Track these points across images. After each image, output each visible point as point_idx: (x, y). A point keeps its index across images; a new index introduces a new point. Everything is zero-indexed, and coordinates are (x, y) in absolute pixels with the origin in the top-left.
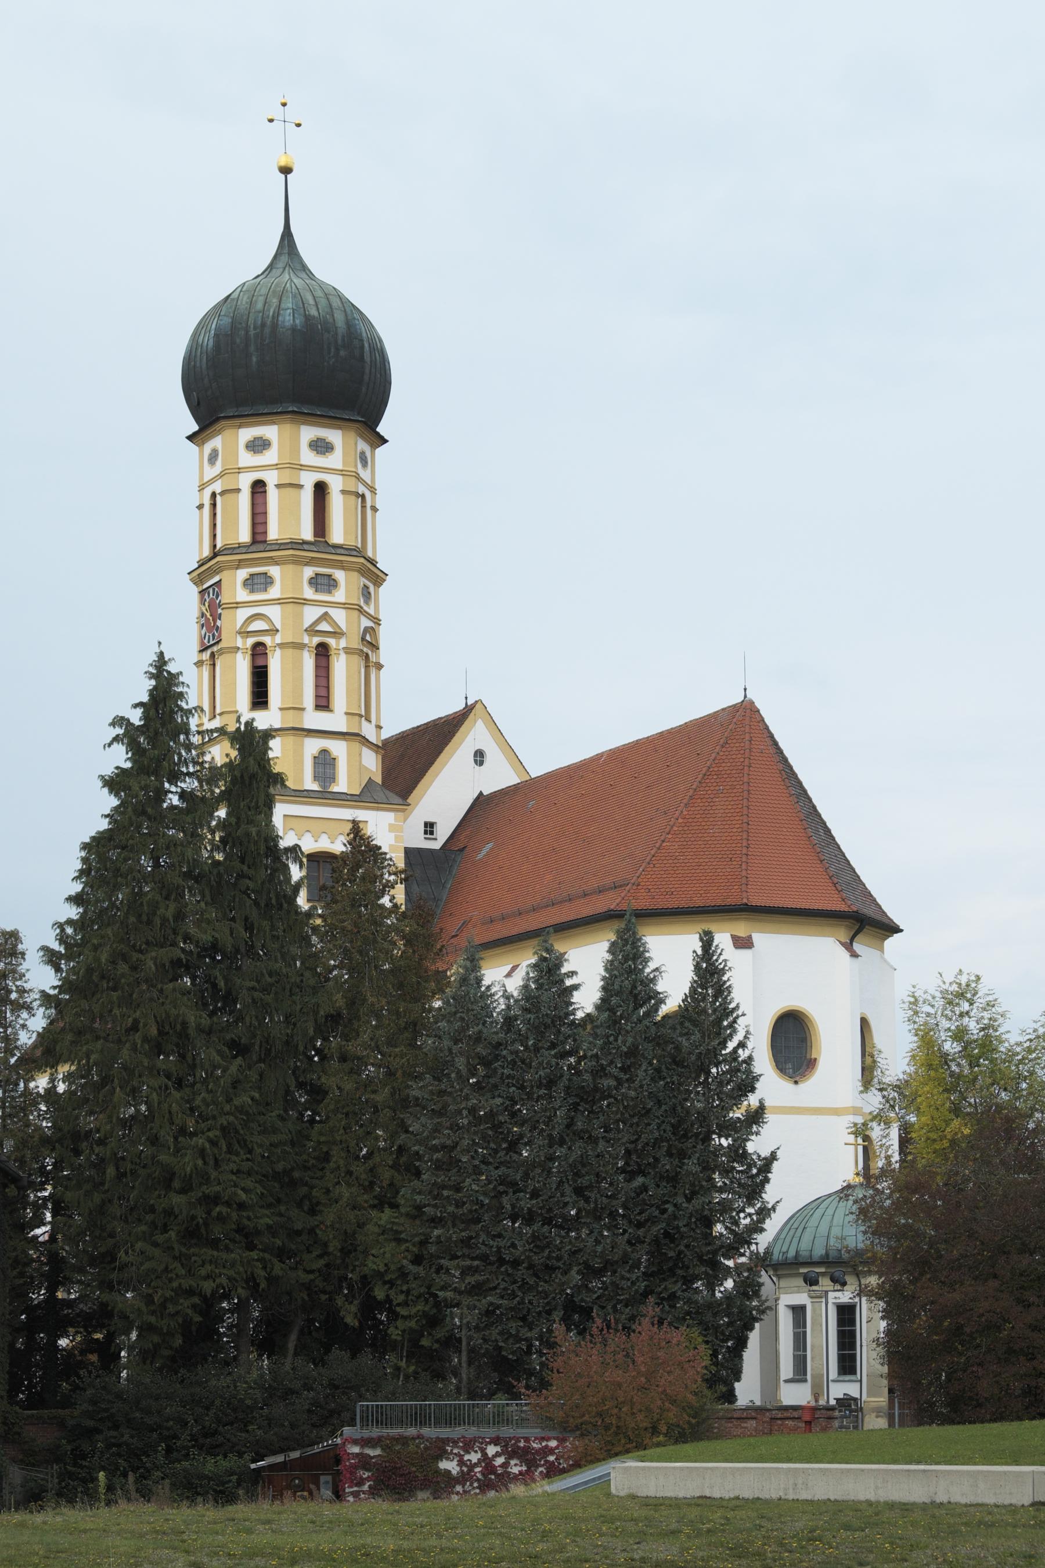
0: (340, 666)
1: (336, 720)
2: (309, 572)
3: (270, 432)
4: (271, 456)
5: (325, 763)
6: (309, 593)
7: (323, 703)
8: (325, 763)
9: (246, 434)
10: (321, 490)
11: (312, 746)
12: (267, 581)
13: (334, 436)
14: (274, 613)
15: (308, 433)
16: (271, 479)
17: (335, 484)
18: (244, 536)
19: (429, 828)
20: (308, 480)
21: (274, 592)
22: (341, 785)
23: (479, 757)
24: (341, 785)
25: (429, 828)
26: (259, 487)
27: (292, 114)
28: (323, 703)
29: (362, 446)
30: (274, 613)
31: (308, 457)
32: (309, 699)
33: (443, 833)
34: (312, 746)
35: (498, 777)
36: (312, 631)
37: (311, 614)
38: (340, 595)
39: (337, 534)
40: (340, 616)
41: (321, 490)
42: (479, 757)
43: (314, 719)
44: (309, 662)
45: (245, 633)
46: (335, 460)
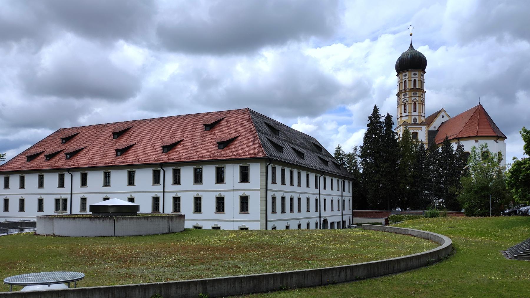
0: (417, 106)
1: (417, 113)
2: (413, 93)
3: (407, 73)
4: (407, 77)
5: (415, 120)
6: (413, 96)
7: (415, 111)
8: (415, 120)
9: (404, 74)
10: (415, 81)
11: (413, 117)
12: (407, 94)
13: (417, 73)
14: (407, 99)
15: (413, 73)
16: (407, 80)
17: (417, 79)
18: (403, 89)
19: (435, 127)
20: (413, 79)
21: (407, 96)
22: (418, 122)
23: (443, 117)
24: (418, 122)
25: (435, 127)
26: (405, 81)
27: (412, 27)
28: (415, 111)
29: (422, 73)
30: (407, 99)
31: (413, 76)
32: (412, 110)
33: (437, 128)
34: (413, 117)
35: (446, 119)
36: (413, 101)
37: (413, 99)
38: (418, 95)
39: (417, 87)
40: (417, 98)
41: (415, 81)
42: (443, 117)
43: (413, 113)
44: (413, 105)
45: (403, 102)
46: (417, 76)
